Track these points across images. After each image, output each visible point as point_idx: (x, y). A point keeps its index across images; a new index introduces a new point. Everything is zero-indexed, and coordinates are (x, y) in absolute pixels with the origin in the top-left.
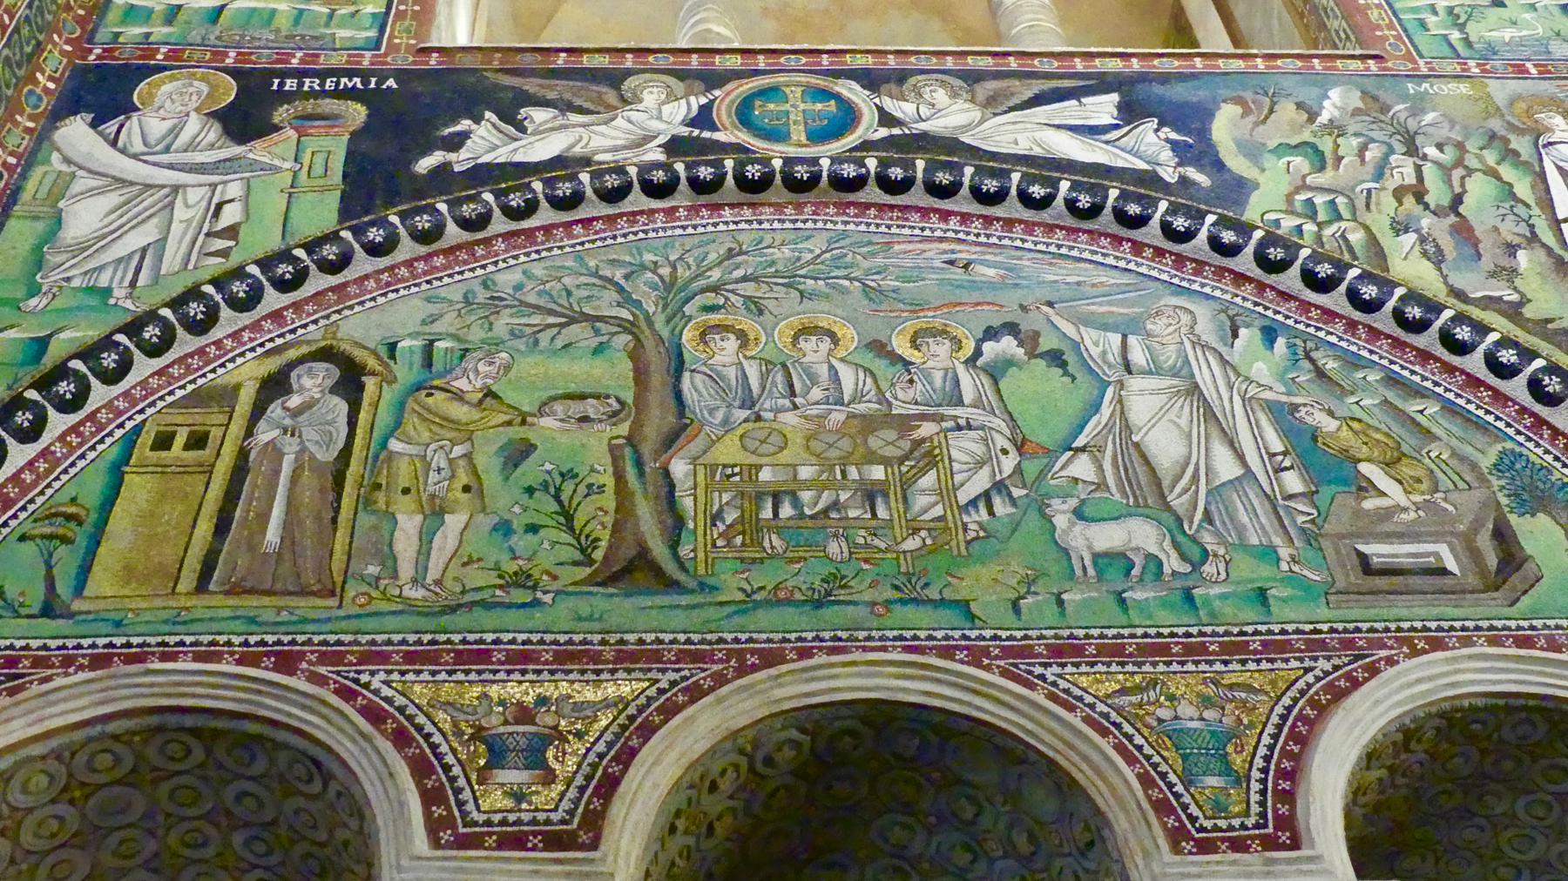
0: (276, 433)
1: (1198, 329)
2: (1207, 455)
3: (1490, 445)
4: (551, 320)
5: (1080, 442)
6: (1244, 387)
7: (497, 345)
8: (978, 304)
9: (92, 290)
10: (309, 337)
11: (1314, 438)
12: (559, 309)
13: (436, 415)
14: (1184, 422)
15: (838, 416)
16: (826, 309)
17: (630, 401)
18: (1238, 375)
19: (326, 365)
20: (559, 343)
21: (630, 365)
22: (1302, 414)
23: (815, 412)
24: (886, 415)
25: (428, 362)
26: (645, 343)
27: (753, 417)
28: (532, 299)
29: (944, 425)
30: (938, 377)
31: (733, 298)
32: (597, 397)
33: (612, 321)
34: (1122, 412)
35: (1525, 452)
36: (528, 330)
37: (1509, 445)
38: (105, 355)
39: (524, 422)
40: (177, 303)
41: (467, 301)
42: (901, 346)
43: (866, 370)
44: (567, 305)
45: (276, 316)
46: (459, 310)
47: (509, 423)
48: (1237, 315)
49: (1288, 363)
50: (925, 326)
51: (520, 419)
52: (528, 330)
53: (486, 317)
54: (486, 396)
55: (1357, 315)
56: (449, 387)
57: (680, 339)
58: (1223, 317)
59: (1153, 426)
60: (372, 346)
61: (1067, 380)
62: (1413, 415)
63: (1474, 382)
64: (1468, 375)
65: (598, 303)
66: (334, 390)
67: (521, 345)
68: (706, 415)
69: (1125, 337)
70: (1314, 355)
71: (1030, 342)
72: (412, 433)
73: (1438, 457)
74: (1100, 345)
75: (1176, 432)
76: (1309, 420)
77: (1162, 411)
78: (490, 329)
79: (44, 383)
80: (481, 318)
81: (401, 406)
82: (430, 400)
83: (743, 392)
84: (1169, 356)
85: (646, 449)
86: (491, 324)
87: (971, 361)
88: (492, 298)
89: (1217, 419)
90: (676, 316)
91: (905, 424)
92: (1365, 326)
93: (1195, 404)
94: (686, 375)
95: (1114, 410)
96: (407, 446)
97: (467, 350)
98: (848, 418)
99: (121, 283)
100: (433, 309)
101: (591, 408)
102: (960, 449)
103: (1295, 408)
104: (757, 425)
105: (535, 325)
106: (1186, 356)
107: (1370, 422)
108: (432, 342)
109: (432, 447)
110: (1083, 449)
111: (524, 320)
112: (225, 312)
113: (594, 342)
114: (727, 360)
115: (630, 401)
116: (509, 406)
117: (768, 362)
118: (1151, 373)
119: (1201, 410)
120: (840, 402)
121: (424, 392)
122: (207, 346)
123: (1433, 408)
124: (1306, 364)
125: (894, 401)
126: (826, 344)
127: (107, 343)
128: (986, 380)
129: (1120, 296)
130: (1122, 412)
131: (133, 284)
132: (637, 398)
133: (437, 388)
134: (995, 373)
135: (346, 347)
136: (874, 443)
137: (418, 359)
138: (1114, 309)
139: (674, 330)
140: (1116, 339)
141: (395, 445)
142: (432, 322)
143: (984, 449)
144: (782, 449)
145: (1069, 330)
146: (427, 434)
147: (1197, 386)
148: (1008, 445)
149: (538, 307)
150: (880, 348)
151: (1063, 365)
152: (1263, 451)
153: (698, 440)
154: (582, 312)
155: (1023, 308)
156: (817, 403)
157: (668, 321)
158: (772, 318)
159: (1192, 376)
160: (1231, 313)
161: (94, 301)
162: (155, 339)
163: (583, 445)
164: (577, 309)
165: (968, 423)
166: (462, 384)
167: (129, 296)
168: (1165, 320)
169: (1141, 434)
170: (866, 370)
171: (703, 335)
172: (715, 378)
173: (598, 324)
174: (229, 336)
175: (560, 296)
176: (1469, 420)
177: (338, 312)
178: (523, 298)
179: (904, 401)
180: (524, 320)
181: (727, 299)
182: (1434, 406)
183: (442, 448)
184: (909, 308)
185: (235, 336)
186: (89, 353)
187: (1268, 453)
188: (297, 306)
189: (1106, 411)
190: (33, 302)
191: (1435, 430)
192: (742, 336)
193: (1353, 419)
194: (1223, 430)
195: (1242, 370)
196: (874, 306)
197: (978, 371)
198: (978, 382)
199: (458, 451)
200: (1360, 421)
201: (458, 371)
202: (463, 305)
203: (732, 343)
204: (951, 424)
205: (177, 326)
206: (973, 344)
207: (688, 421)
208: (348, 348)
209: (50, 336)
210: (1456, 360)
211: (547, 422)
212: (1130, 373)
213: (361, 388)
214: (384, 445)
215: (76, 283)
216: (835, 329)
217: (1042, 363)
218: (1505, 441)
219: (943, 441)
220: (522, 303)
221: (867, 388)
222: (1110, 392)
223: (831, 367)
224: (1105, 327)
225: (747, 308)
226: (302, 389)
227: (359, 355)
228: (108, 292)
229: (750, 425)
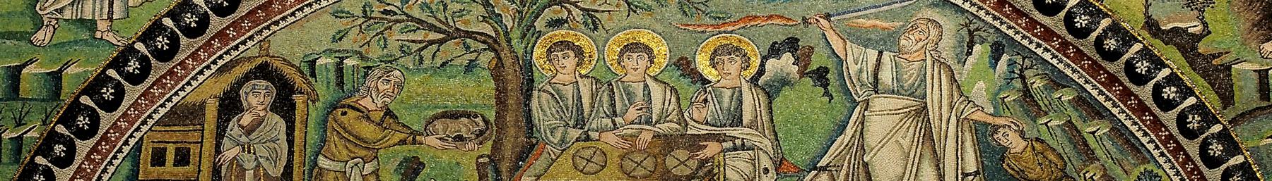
0: (237, 150)
1: (941, 45)
2: (916, 175)
3: (1135, 166)
4: (433, 36)
5: (823, 163)
6: (963, 107)
7: (391, 62)
8: (770, 17)
9: (81, 22)
10: (249, 53)
11: (1002, 159)
12: (438, 24)
13: (350, 134)
14: (906, 143)
15: (647, 136)
16: (647, 23)
17: (492, 120)
18: (961, 95)
19: (264, 83)
20: (439, 62)
21: (492, 84)
22: (1000, 135)
23: (629, 132)
24: (682, 136)
25: (340, 83)
26: (504, 60)
27: (583, 137)
28: (416, 13)
29: (724, 144)
30: (728, 93)
31: (575, 12)
32: (468, 116)
33: (479, 37)
34: (862, 133)
35: (1160, 172)
36: (415, 47)
37: (1150, 167)
38: (104, 90)
39: (414, 142)
40: (147, 37)
41: (367, 17)
42: (702, 64)
43: (673, 89)
44: (444, 20)
45: (221, 35)
46: (360, 26)
47: (403, 142)
48: (977, 29)
49: (1004, 82)
50: (724, 42)
51: (411, 138)
52: (415, 47)
53: (382, 33)
54: (386, 114)
55: (1069, 38)
56: (357, 106)
57: (531, 58)
58: (965, 32)
59: (882, 147)
60: (297, 63)
61: (827, 99)
62: (1086, 136)
63: (1142, 109)
64: (1140, 100)
65: (468, 17)
66: (274, 108)
67: (409, 62)
68: (549, 135)
69: (881, 53)
70: (1026, 73)
71: (803, 60)
72: (335, 150)
73: (1091, 177)
74: (858, 60)
75: (899, 153)
76: (1003, 142)
77: (895, 130)
78: (385, 47)
79: (67, 119)
80: (377, 34)
81: (323, 124)
82: (344, 119)
83: (578, 110)
84: (910, 75)
85: (504, 167)
86: (385, 40)
87: (754, 81)
88: (385, 12)
89: (933, 140)
90: (529, 32)
91: (695, 143)
92: (1074, 47)
93: (920, 124)
94: (535, 93)
95: (855, 131)
96: (331, 163)
97: (369, 68)
98: (654, 136)
99: (101, 15)
100: (341, 24)
101: (463, 126)
102: (734, 168)
103: (996, 128)
104: (588, 144)
105: (420, 42)
106: (926, 73)
107: (1051, 143)
108: (342, 59)
109: (350, 163)
110: (823, 169)
111: (411, 36)
112: (184, 40)
113: (465, 61)
114: (568, 78)
115: (492, 120)
116: (404, 126)
117: (598, 81)
118: (893, 92)
119: (923, 130)
120: (648, 122)
121: (340, 111)
122: (174, 67)
123: (1103, 128)
124: (1018, 84)
125: (693, 123)
126: (643, 63)
127: (102, 80)
128: (762, 97)
129: (886, 8)
130: (862, 133)
131: (110, 18)
132: (499, 116)
133: (350, 107)
134: (769, 94)
135: (276, 64)
136: (670, 162)
137: (332, 76)
138: (878, 22)
139: (526, 48)
140: (872, 54)
141: (323, 162)
142: (340, 39)
143: (751, 168)
144: (603, 167)
145: (837, 44)
146: (345, 152)
147: (925, 107)
148: (769, 165)
149: (420, 21)
150: (684, 66)
151: (825, 86)
152: (960, 171)
153: (542, 158)
154: (457, 29)
155: (805, 20)
156: (632, 123)
157: (524, 36)
158: (605, 35)
159: (924, 97)
160: (972, 27)
161: (85, 35)
162: (137, 71)
163: (458, 164)
164: (452, 24)
165: (743, 144)
166: (366, 103)
167: (110, 30)
168: (917, 35)
169: (871, 154)
170: (673, 89)
171: (549, 51)
172: (557, 97)
173: (468, 40)
174: (189, 56)
175: (438, 9)
176: (1128, 141)
177: (268, 28)
178: (410, 13)
179: (700, 118)
180: (411, 36)
181: (569, 11)
182: (1106, 127)
183: (356, 165)
184: (713, 22)
185: (194, 56)
186: (93, 89)
187: (962, 173)
188: (234, 24)
189: (849, 131)
190: (40, 35)
191: (1099, 152)
192: (579, 52)
193: (1037, 140)
194: (935, 152)
195: (964, 89)
196: (685, 20)
197: (759, 91)
198: (757, 102)
199: (369, 168)
200: (1042, 142)
201: (363, 90)
202: (363, 20)
203: (570, 61)
204: (729, 145)
205: (151, 58)
206: (760, 60)
207: (534, 141)
208: (279, 65)
209: (60, 71)
210: (1133, 88)
211: (432, 140)
212: (876, 92)
213: (293, 106)
214: (316, 164)
215: (67, 14)
216: (652, 45)
217: (808, 81)
218: (1149, 162)
219: (721, 158)
220: (413, 19)
221: (671, 109)
222: (858, 109)
223: (646, 86)
224: (867, 43)
225: (586, 24)
226: (249, 105)
227: (287, 71)
228: (91, 25)
229: (581, 143)
